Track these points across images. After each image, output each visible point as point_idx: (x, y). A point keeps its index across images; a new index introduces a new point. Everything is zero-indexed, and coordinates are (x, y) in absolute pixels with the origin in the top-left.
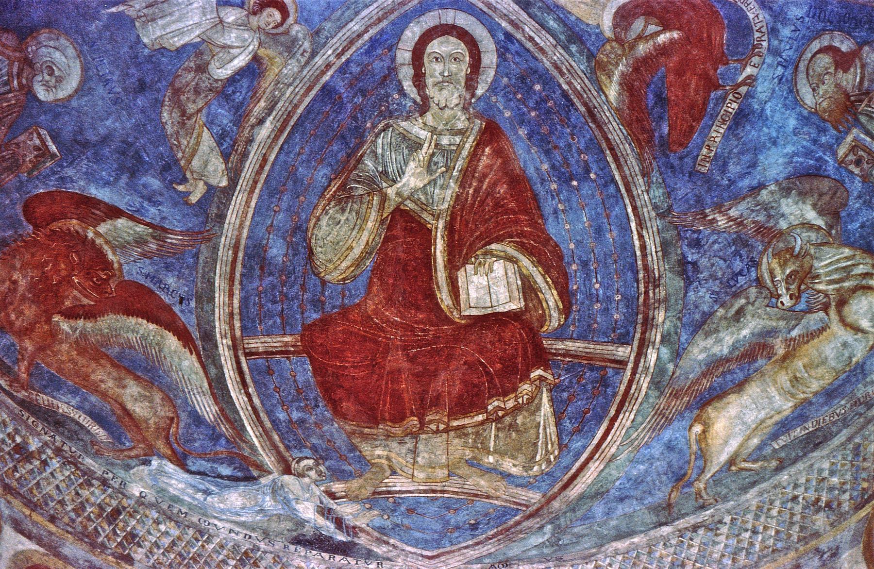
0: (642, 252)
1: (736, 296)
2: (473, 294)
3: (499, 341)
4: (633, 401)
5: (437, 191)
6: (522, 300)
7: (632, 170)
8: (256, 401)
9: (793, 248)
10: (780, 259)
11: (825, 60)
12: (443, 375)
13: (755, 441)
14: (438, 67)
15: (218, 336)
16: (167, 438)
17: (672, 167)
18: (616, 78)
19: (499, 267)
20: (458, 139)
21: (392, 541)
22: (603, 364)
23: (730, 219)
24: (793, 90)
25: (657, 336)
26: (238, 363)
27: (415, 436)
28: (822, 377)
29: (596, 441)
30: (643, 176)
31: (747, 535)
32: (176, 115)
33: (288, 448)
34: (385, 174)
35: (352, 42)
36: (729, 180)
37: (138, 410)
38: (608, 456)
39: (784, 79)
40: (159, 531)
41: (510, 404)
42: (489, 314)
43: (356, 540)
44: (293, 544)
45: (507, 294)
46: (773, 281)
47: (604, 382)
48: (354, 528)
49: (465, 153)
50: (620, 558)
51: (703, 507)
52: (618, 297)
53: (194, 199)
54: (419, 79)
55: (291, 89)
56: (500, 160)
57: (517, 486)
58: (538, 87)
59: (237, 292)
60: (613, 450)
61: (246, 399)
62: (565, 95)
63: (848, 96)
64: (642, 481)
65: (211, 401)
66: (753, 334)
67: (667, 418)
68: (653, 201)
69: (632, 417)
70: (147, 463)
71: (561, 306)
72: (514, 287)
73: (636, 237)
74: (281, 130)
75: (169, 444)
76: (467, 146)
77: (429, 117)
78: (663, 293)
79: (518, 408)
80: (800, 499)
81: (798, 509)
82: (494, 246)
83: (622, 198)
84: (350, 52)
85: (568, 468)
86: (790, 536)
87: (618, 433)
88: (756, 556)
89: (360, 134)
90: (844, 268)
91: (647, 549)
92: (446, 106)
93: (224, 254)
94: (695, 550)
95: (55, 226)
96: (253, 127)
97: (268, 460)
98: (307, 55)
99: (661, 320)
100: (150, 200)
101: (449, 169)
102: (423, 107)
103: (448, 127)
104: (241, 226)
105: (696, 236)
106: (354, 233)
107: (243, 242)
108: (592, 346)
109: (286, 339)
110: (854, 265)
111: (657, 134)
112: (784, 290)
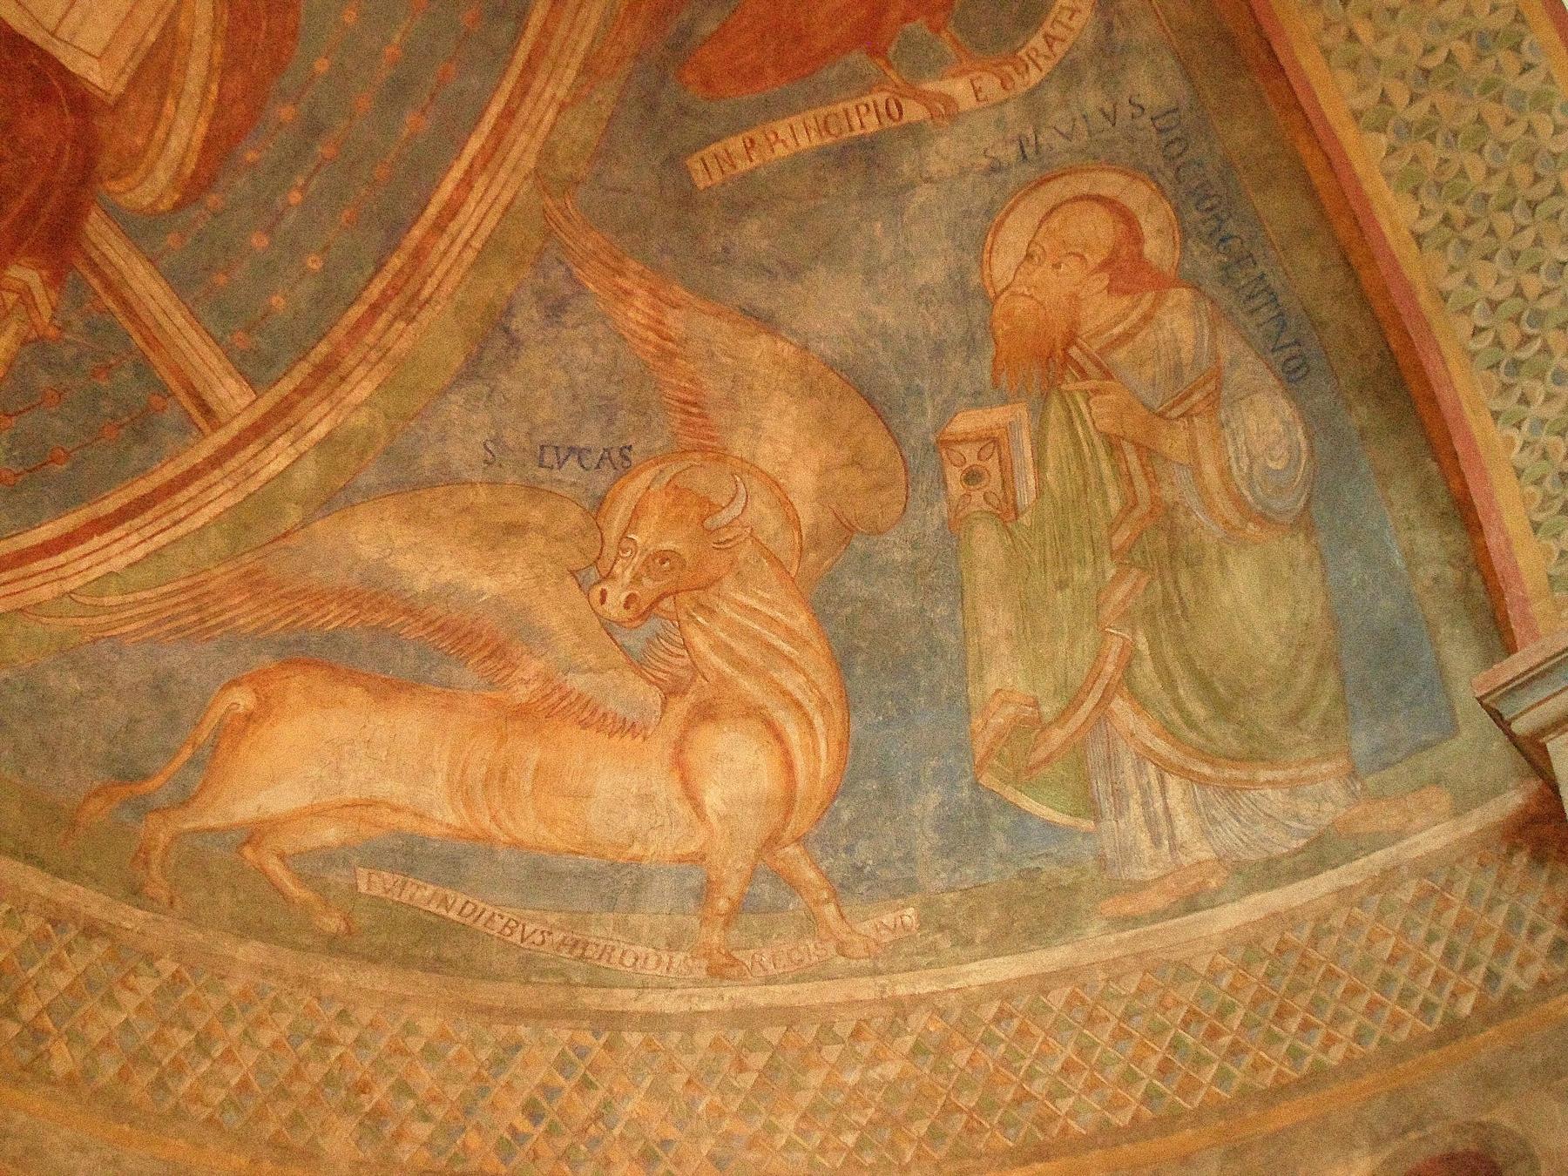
0: (440, 215)
1: (533, 490)
4: (166, 522)
6: (124, 79)
7: (575, 36)
9: (714, 509)
10: (674, 505)
11: (1098, 229)
13: (330, 834)
17: (652, 108)
22: (173, 384)
23: (657, 326)
24: (992, 219)
25: (320, 422)
28: (552, 822)
31: (184, 1039)
36: (726, 250)
39: (998, 177)
42: (32, 44)
45: (107, 35)
46: (624, 536)
51: (135, 893)
52: (314, 263)
60: (46, 593)
63: (1071, 339)
64: (54, 714)
66: (498, 602)
67: (202, 621)
68: (555, 137)
69: (139, 553)
71: (188, 172)
72: (132, 36)
73: (457, 173)
78: (404, 344)
80: (335, 1053)
81: (315, 1071)
83: (504, 72)
86: (260, 1116)
88: (171, 1101)
90: (769, 646)
94: (62, 980)
105: (567, 290)
108: (180, 321)
110: (791, 661)
111: (685, 16)
112: (628, 573)
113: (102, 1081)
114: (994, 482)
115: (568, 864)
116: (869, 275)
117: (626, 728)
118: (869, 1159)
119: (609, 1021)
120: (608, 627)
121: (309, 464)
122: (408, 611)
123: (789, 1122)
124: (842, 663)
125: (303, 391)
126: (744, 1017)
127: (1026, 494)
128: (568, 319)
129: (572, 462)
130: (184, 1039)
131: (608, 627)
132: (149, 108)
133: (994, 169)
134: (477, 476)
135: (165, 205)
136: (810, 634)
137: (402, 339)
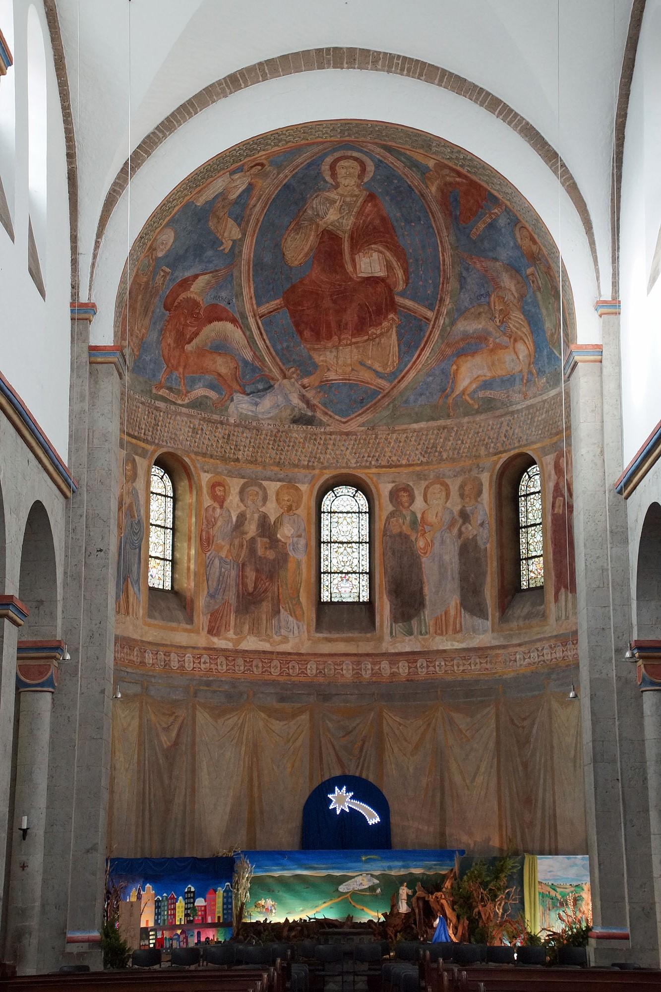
1: (480, 305)
2: (363, 266)
3: (375, 293)
5: (344, 221)
8: (267, 342)
9: (504, 298)
12: (349, 312)
13: (474, 386)
14: (343, 171)
16: (236, 379)
18: (436, 184)
19: (375, 255)
20: (355, 199)
21: (329, 413)
23: (482, 266)
25: (445, 311)
26: (257, 324)
27: (337, 348)
30: (446, 229)
32: (215, 220)
33: (284, 364)
34: (318, 215)
38: (418, 369)
41: (379, 332)
44: (291, 423)
47: (421, 329)
48: (314, 405)
49: (358, 204)
50: (416, 433)
51: (449, 416)
53: (227, 251)
54: (334, 175)
56: (376, 209)
57: (380, 378)
60: (420, 366)
61: (263, 343)
62: (409, 186)
65: (249, 349)
69: (430, 351)
70: (232, 400)
72: (383, 265)
73: (441, 255)
74: (265, 207)
78: (450, 289)
81: (478, 439)
82: (373, 246)
84: (296, 171)
85: (401, 371)
87: (423, 358)
89: (304, 200)
91: (426, 432)
93: (244, 269)
94: (442, 440)
95: (176, 304)
96: (251, 209)
97: (276, 373)
98: (275, 175)
99: (447, 303)
100: (210, 262)
101: (350, 212)
102: (337, 186)
104: (250, 253)
106: (304, 242)
107: (252, 260)
108: (416, 305)
109: (276, 302)
113: (450, 456)
117: (507, 347)
118: (542, 436)
119: (512, 413)
120: (499, 327)
121: (446, 319)
123: (534, 430)
124: (529, 324)
126: (528, 407)
127: (541, 285)
128: (470, 270)
130: (460, 442)
131: (499, 327)
133: (509, 224)
134: (471, 307)
136: (523, 319)
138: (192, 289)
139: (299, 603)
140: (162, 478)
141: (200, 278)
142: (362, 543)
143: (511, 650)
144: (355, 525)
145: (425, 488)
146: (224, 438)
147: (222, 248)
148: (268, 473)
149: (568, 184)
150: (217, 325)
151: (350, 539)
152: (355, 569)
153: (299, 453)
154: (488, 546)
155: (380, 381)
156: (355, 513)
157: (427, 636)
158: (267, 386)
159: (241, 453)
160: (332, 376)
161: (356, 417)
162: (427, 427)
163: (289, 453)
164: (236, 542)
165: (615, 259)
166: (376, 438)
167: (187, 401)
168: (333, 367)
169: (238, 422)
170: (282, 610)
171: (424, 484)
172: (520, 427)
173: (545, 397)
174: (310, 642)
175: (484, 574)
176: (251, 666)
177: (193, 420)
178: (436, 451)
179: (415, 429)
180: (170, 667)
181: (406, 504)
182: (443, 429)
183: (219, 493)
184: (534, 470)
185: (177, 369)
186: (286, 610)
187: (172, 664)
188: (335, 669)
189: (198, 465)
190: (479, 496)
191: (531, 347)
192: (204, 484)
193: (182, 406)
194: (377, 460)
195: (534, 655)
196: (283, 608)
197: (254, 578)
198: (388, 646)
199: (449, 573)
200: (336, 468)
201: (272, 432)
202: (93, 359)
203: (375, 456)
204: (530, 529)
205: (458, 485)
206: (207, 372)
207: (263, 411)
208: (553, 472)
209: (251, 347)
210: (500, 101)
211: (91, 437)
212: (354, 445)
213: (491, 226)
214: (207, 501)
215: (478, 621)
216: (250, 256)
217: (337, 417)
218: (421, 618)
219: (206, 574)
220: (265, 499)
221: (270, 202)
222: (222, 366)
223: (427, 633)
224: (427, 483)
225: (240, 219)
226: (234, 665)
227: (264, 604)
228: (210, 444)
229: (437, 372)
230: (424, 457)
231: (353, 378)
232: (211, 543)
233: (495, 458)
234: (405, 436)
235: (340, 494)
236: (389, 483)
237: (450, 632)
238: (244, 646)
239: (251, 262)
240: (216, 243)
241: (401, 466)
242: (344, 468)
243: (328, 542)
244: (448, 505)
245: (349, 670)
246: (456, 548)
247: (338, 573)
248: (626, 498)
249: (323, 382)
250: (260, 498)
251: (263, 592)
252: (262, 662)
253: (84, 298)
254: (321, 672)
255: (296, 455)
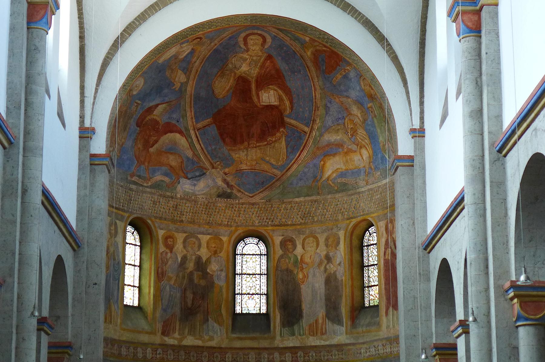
1: (338, 125)
2: (264, 98)
8: (202, 145)
13: (334, 175)
14: (252, 42)
15: (189, 127)
16: (182, 170)
18: (310, 51)
19: (272, 92)
20: (259, 58)
21: (242, 190)
23: (340, 101)
26: (196, 134)
29: (296, 157)
30: (317, 77)
31: (325, 211)
33: (212, 159)
34: (235, 67)
35: (223, 39)
37: (173, 164)
38: (299, 163)
40: (186, 207)
41: (274, 139)
43: (233, 191)
44: (217, 197)
47: (300, 138)
48: (232, 186)
50: (297, 204)
51: (318, 194)
52: (307, 109)
53: (177, 89)
54: (246, 43)
55: (204, 52)
57: (275, 168)
58: (285, 48)
59: (193, 110)
62: (294, 51)
69: (306, 152)
70: (179, 183)
72: (276, 98)
73: (313, 92)
74: (201, 63)
75: (182, 171)
76: (262, 60)
77: (249, 53)
79: (275, 141)
81: (337, 209)
82: (270, 86)
84: (222, 41)
92: (255, 50)
93: (188, 100)
95: (144, 123)
97: (207, 165)
99: (318, 122)
100: (165, 96)
102: (248, 50)
103: (256, 55)
104: (192, 90)
108: (298, 124)
109: (208, 120)
114: (373, 112)
115: (355, 171)
116: (353, 89)
117: (355, 151)
119: (359, 193)
121: (317, 132)
122: (333, 145)
123: (372, 204)
124: (370, 138)
125: (313, 124)
126: (369, 190)
129: (340, 120)
130: (325, 211)
132: (283, 103)
133: (356, 76)
135: (290, 111)
137: (319, 113)
138: (154, 113)
139: (221, 315)
140: (133, 233)
141: (159, 106)
142: (262, 274)
143: (358, 346)
144: (258, 263)
145: (303, 241)
146: (173, 207)
147: (174, 88)
148: (202, 229)
149: (392, 56)
150: (170, 136)
151: (254, 272)
152: (258, 292)
153: (222, 217)
154: (344, 278)
155: (274, 170)
156: (258, 255)
157: (304, 337)
158: (201, 173)
159: (184, 216)
160: (244, 167)
161: (259, 193)
162: (305, 201)
163: (215, 216)
164: (181, 274)
165: (422, 103)
166: (272, 207)
167: (150, 184)
168: (245, 162)
169: (183, 196)
170: (210, 319)
171: (302, 237)
172: (364, 202)
173: (380, 184)
174: (228, 340)
175: (341, 296)
176: (190, 356)
177: (154, 196)
178: (310, 216)
179: (297, 201)
180: (137, 357)
181: (291, 250)
182: (315, 202)
183: (170, 243)
184: (372, 229)
185: (144, 164)
186: (213, 319)
187: (138, 355)
188: (244, 357)
189: (157, 225)
190: (338, 246)
191: (371, 152)
192: (160, 238)
193: (147, 187)
194: (272, 221)
195: (373, 350)
196: (210, 317)
197: (192, 297)
198: (278, 342)
199: (318, 296)
200: (246, 226)
201: (204, 203)
202: (92, 162)
203: (271, 219)
204: (370, 268)
205: (325, 238)
206: (163, 165)
207: (199, 189)
208: (384, 232)
209: (192, 150)
210: (350, 5)
211: (90, 211)
212: (257, 211)
213: (346, 77)
214: (162, 248)
215: (337, 327)
216: (192, 92)
217: (246, 193)
218: (300, 325)
219: (161, 296)
220: (200, 246)
221: (205, 60)
222: (173, 161)
223: (304, 334)
224: (304, 236)
225: (187, 71)
226: (178, 356)
227: (198, 315)
228: (164, 211)
229: (311, 166)
230: (303, 220)
231: (257, 168)
232: (164, 275)
233: (348, 221)
234: (290, 206)
235: (248, 242)
236: (280, 236)
237: (319, 334)
238: (185, 342)
239: (193, 96)
240: (170, 84)
241: (288, 225)
242: (251, 226)
243: (240, 274)
244: (318, 251)
245: (253, 358)
246: (323, 279)
247: (247, 294)
248: (429, 253)
249: (238, 171)
250: (196, 245)
251: (197, 308)
252: (196, 353)
253: (87, 124)
254: (234, 360)
255: (220, 218)
